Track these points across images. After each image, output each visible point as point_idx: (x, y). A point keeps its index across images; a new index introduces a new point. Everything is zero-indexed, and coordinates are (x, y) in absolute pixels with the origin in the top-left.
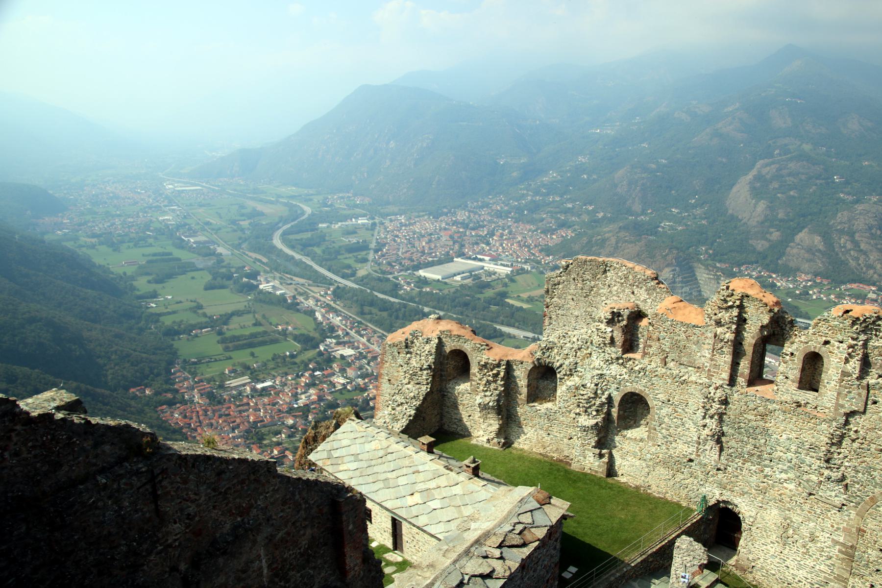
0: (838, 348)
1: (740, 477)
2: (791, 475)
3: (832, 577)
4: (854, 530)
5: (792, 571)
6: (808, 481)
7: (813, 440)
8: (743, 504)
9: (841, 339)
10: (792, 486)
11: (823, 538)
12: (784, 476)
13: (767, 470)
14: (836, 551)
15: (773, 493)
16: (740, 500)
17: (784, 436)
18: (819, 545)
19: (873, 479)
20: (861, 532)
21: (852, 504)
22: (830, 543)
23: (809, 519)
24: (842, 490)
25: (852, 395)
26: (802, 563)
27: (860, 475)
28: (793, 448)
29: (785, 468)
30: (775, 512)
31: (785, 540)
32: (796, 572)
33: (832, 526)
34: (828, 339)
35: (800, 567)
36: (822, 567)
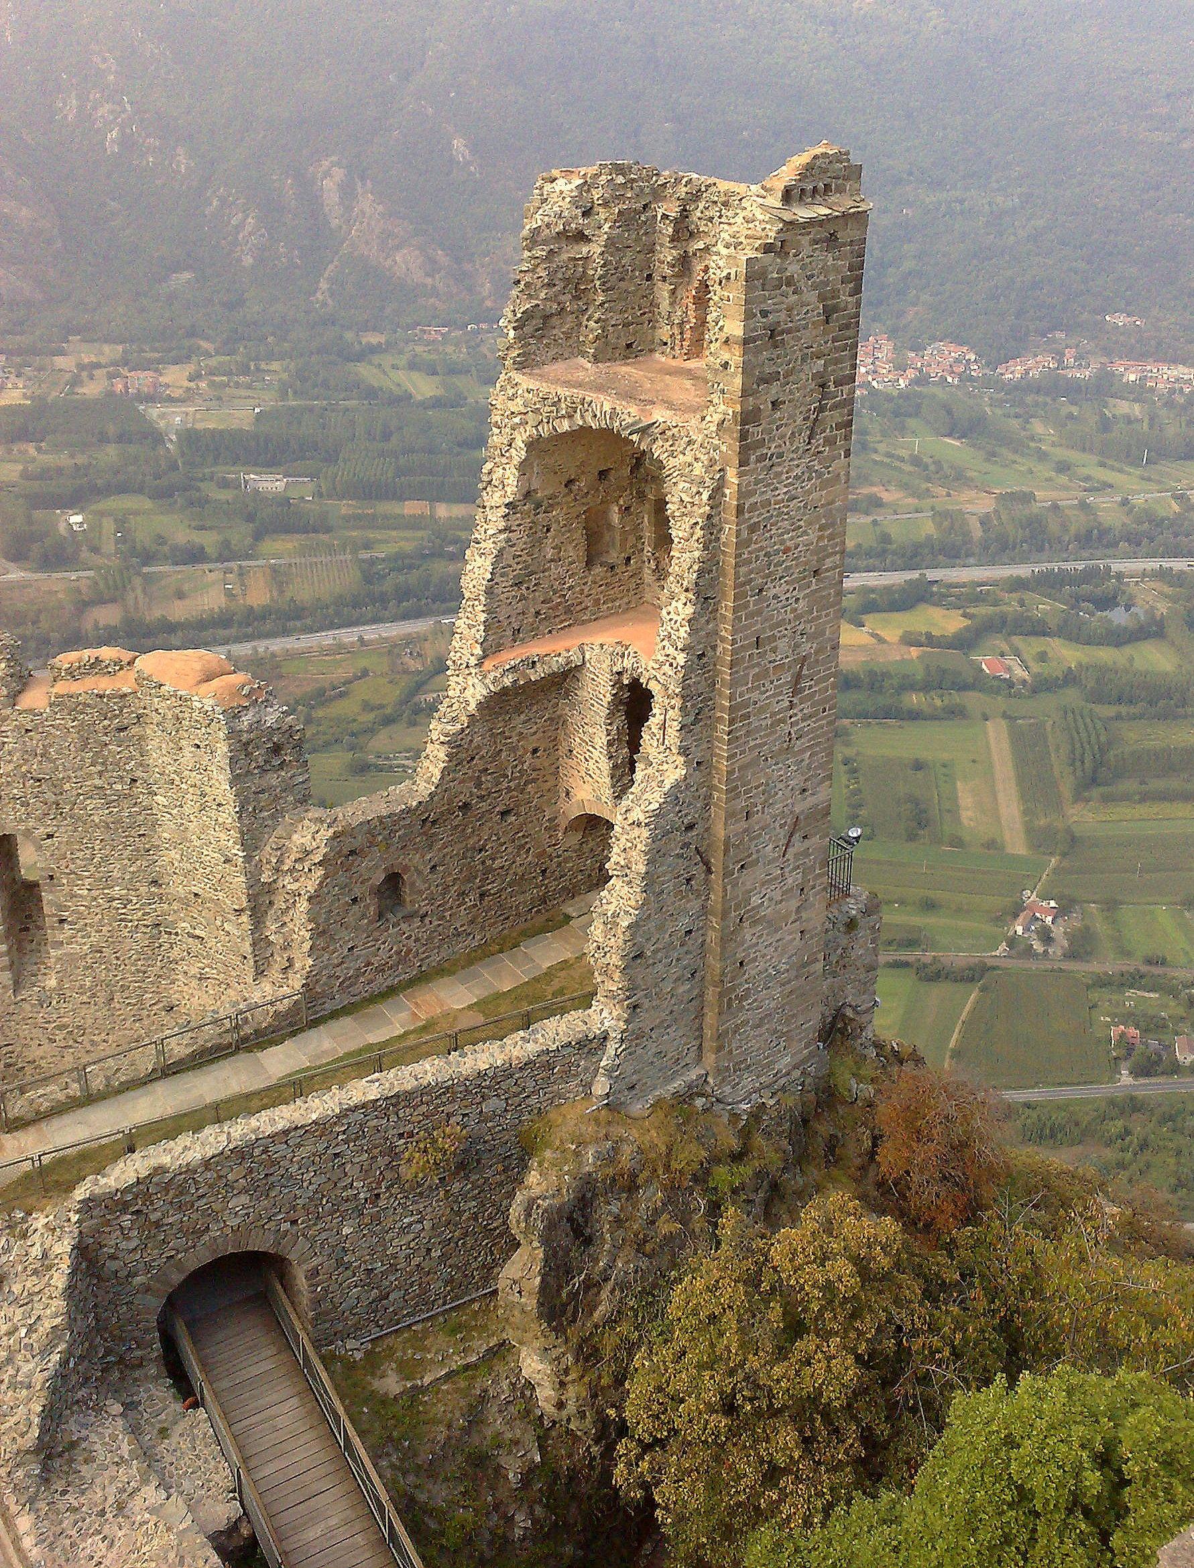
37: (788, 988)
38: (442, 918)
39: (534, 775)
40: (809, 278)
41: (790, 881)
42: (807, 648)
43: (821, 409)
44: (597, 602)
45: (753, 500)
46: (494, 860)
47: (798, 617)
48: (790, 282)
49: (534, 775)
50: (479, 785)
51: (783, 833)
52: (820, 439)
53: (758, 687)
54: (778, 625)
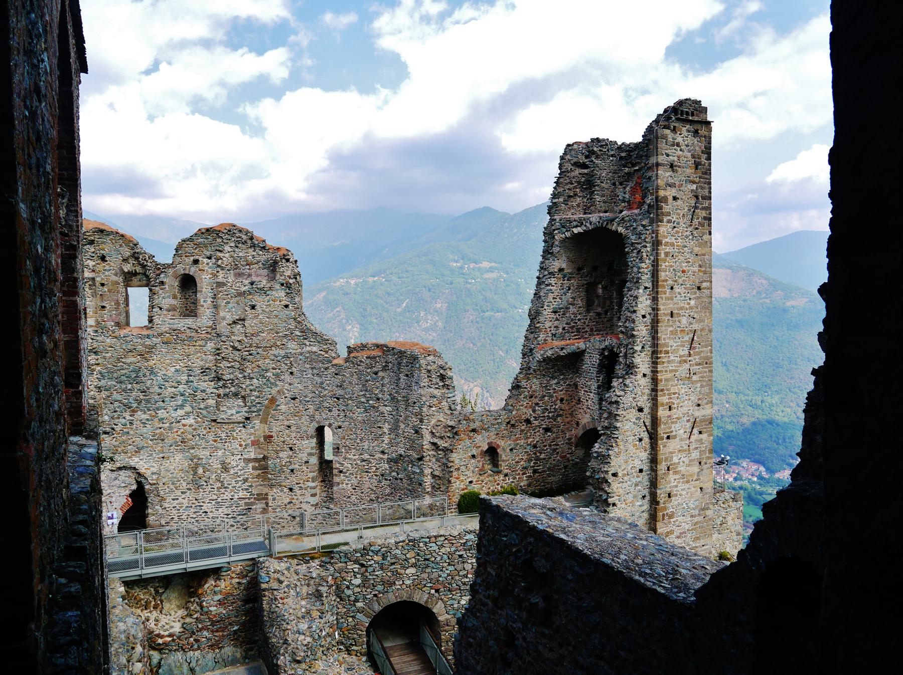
0: (208, 264)
1: (131, 432)
2: (188, 408)
3: (252, 500)
4: (262, 440)
5: (211, 515)
6: (206, 408)
7: (202, 363)
8: (141, 463)
9: (208, 254)
10: (190, 421)
11: (233, 461)
12: (180, 412)
13: (162, 413)
14: (251, 470)
15: (171, 437)
16: (137, 460)
17: (173, 369)
18: (232, 472)
19: (268, 380)
20: (268, 438)
21: (254, 414)
22: (242, 464)
23: (217, 448)
24: (242, 404)
25: (230, 305)
26: (219, 500)
27: (255, 381)
28: (184, 378)
29: (180, 403)
30: (179, 457)
31: (196, 484)
32: (216, 513)
33: (241, 445)
34: (197, 257)
35: (218, 505)
36: (241, 494)
37: (696, 519)
38: (515, 478)
39: (561, 412)
40: (687, 146)
41: (693, 455)
42: (695, 326)
43: (696, 207)
44: (592, 330)
45: (667, 240)
46: (541, 453)
47: (691, 308)
48: (678, 145)
49: (561, 412)
50: (534, 411)
51: (689, 425)
52: (696, 222)
53: (673, 339)
54: (682, 308)
